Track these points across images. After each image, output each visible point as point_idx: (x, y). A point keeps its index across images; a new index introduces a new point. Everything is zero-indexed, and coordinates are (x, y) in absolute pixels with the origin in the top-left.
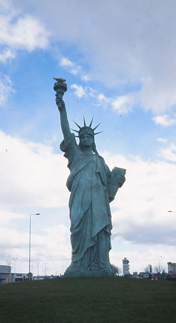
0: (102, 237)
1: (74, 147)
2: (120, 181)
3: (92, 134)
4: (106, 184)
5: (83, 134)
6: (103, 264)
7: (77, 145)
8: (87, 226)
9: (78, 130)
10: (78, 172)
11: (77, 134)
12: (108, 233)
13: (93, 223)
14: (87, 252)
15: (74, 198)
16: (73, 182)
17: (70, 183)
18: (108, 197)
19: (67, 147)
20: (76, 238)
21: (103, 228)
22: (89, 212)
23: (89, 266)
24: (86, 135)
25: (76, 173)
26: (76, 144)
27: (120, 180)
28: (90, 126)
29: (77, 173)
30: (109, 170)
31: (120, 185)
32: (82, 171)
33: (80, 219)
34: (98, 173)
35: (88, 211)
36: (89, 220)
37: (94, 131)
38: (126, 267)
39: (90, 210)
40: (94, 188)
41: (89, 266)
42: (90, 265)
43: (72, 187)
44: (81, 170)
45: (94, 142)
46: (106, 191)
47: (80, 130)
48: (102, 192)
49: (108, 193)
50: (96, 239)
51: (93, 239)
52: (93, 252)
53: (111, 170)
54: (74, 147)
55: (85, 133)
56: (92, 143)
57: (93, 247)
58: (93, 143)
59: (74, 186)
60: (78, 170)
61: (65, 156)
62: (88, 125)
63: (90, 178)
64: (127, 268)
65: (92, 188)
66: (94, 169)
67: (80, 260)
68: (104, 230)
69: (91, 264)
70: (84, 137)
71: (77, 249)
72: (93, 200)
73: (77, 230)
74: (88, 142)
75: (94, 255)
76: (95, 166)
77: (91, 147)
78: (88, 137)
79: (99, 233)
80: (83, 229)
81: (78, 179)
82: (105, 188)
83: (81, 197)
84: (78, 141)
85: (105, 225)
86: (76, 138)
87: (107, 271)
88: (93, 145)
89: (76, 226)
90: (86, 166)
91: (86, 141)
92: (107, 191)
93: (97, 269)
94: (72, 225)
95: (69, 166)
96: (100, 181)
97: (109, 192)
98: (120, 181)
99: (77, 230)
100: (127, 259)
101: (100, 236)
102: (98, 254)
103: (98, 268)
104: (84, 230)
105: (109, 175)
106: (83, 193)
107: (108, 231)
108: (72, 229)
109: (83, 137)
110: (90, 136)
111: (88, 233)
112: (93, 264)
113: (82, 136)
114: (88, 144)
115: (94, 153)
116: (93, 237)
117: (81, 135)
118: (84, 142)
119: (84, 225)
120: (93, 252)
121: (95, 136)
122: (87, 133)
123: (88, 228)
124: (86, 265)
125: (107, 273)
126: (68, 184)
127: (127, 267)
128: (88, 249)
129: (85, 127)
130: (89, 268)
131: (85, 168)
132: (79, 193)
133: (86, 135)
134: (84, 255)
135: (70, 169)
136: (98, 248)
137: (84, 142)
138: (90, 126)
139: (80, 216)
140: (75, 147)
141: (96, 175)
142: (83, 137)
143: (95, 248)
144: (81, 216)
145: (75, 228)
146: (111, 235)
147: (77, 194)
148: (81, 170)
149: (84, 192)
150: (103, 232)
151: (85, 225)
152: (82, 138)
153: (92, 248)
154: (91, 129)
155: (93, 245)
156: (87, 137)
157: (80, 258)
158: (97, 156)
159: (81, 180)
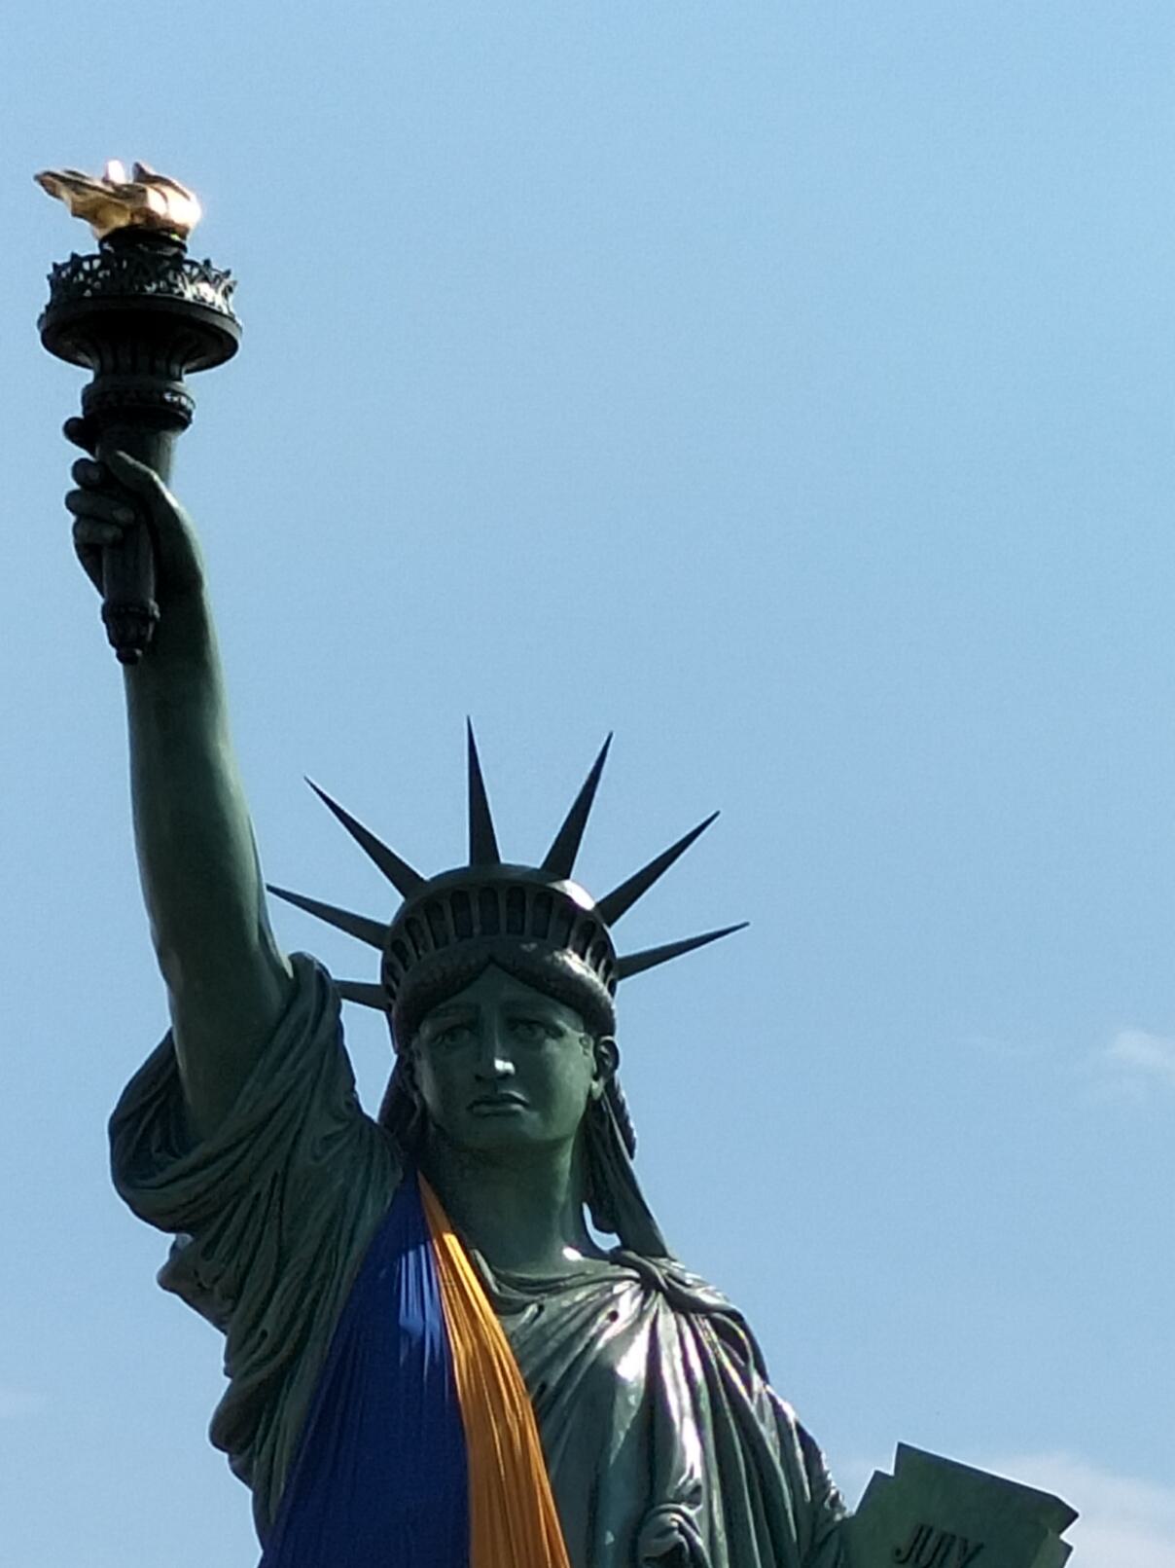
9: (384, 904)
28: (562, 857)
45: (611, 1088)
47: (405, 919)
53: (851, 1504)
61: (174, 1278)
62: (523, 847)
86: (352, 1014)
115: (608, 1242)
121: (631, 1003)
138: (562, 857)
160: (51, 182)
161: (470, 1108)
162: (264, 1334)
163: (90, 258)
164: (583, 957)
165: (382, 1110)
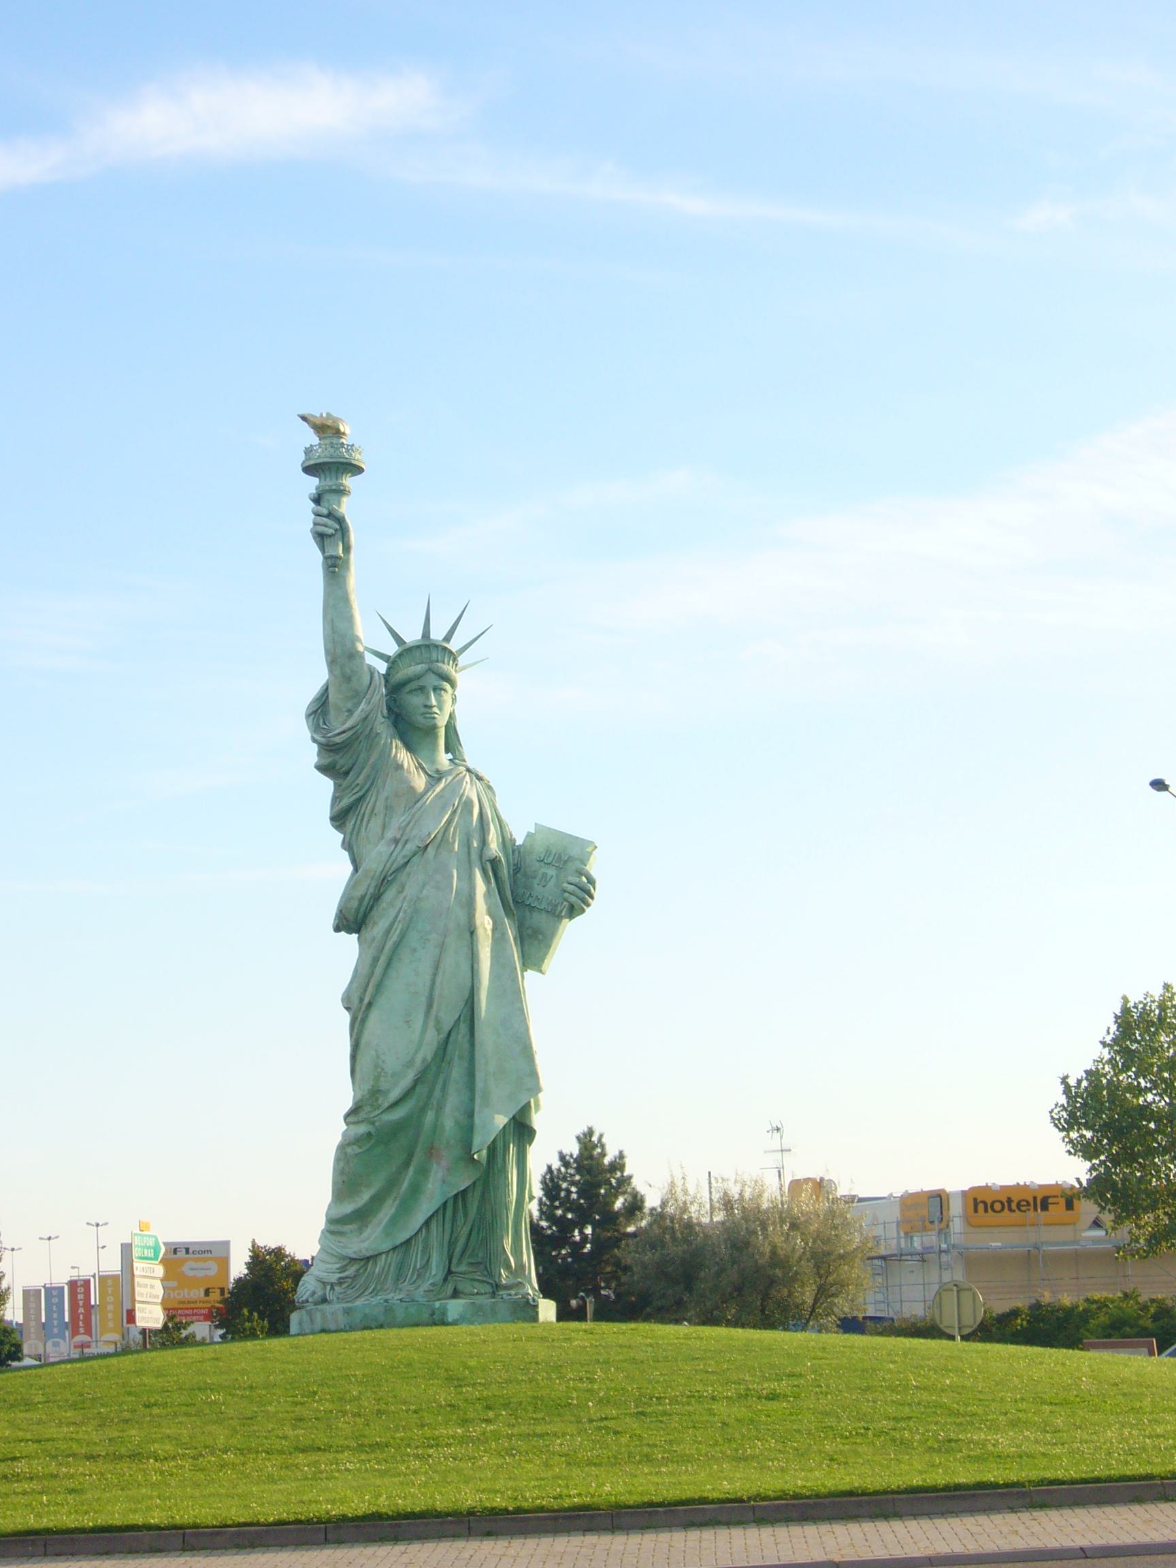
5: (418, 677)
15: (392, 973)
19: (350, 733)
25: (401, 861)
28: (447, 639)
32: (429, 849)
41: (445, 1280)
42: (450, 1272)
47: (400, 655)
52: (466, 1215)
57: (464, 1193)
60: (411, 847)
62: (437, 635)
69: (453, 1269)
75: (466, 1231)
80: (423, 1110)
81: (410, 891)
83: (425, 968)
89: (395, 1094)
104: (430, 1116)
111: (449, 1123)
112: (463, 1268)
113: (413, 685)
119: (430, 1096)
123: (448, 1109)
124: (436, 1271)
130: (449, 1289)
132: (415, 950)
134: (420, 1229)
138: (447, 639)
145: (386, 1105)
151: (437, 1093)
152: (411, 692)
157: (398, 1242)
159: (425, 892)
160: (304, 418)
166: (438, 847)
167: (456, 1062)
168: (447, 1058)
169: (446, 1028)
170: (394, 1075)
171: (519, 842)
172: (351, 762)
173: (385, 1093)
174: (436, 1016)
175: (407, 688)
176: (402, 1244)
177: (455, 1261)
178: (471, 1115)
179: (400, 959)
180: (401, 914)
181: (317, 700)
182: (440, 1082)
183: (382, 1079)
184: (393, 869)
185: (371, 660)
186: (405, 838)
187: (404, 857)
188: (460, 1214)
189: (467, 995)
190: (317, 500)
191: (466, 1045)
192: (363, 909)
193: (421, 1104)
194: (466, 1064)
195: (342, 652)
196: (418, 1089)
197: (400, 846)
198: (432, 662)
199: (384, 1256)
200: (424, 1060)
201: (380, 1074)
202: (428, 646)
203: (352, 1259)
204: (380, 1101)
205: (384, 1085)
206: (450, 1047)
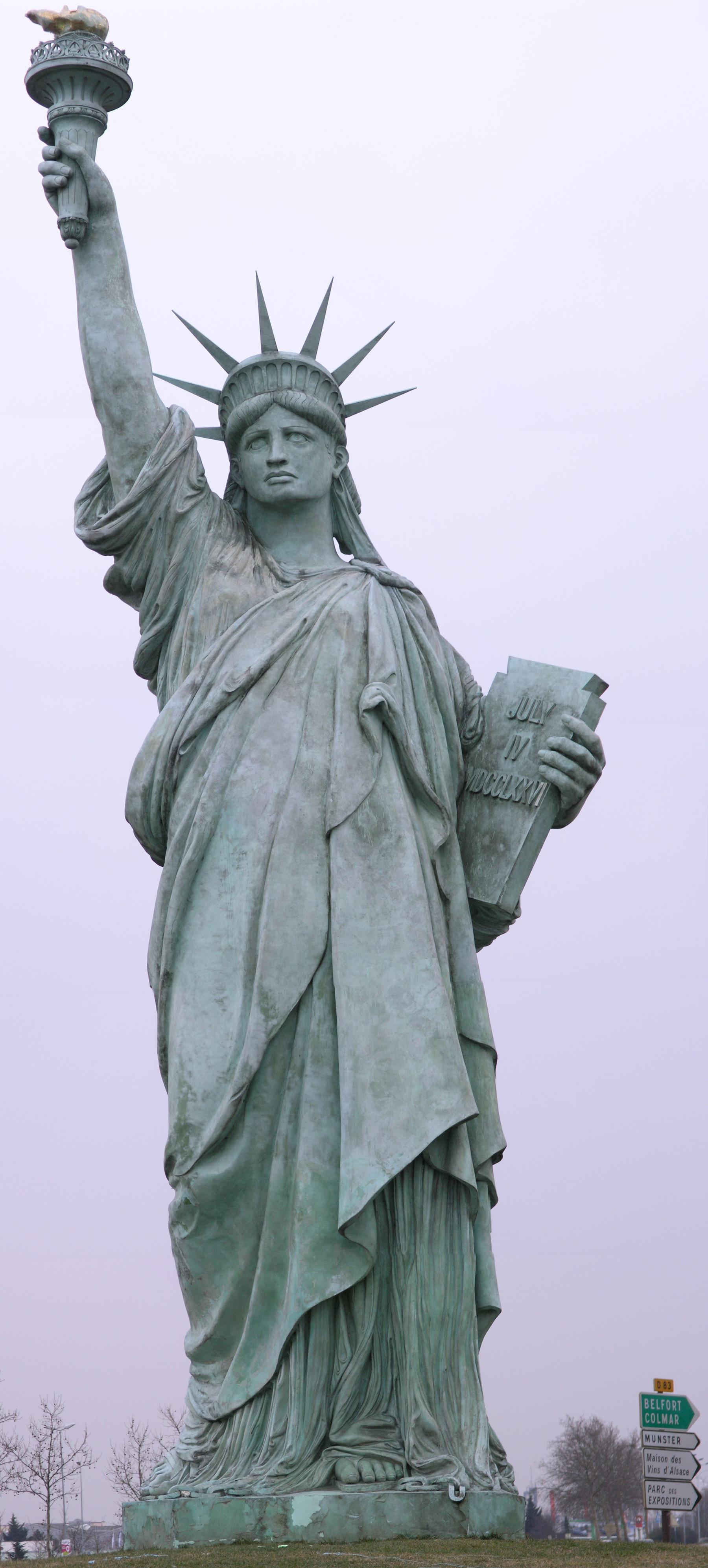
0: (415, 1223)
1: (181, 517)
2: (553, 774)
3: (323, 405)
4: (448, 799)
5: (256, 416)
6: (429, 1433)
7: (214, 496)
8: (296, 1130)
10: (222, 707)
11: (206, 414)
12: (466, 1187)
13: (345, 1106)
14: (301, 1334)
15: (194, 918)
16: (183, 788)
17: (154, 797)
18: (459, 900)
20: (210, 1232)
21: (424, 1145)
22: (314, 1018)
23: (317, 1456)
24: (277, 420)
26: (201, 488)
27: (552, 765)
29: (214, 717)
30: (468, 686)
31: (564, 808)
32: (250, 696)
33: (239, 1078)
34: (379, 710)
35: (302, 1018)
36: (312, 1086)
37: (343, 389)
38: (669, 1454)
39: (318, 1007)
40: (345, 833)
42: (325, 1443)
43: (176, 830)
44: (244, 690)
45: (345, 471)
46: (444, 849)
47: (230, 385)
48: (409, 868)
49: (459, 869)
50: (370, 1235)
51: (345, 1234)
52: (353, 1342)
54: (181, 517)
55: (268, 406)
56: (325, 481)
58: (335, 481)
59: (191, 816)
60: (215, 695)
62: (290, 344)
63: (315, 756)
64: (675, 1460)
65: (328, 836)
66: (348, 675)
67: (250, 1401)
68: (437, 1161)
69: (333, 1438)
70: (265, 436)
71: (224, 1316)
72: (335, 926)
73: (220, 1167)
74: (299, 468)
76: (349, 656)
77: (323, 511)
78: (297, 433)
79: (392, 1185)
82: (438, 832)
83: (241, 903)
84: (215, 463)
85: (436, 1129)
87: (457, 1489)
88: (334, 500)
89: (210, 1131)
90: (280, 663)
91: (283, 462)
92: (457, 857)
93: (380, 1474)
94: (182, 1130)
95: (148, 664)
96: (393, 779)
97: (467, 862)
98: (553, 774)
99: (220, 1167)
100: (677, 1391)
101: (403, 1212)
102: (382, 1358)
103: (388, 1466)
105: (472, 724)
106: (259, 869)
107: (465, 1172)
108: (179, 1159)
109: (256, 439)
110: (313, 430)
111: (304, 1183)
112: (351, 1435)
113: (250, 432)
114: (295, 488)
116: (341, 1223)
117: (243, 425)
118: (267, 471)
119: (273, 1131)
120: (353, 1342)
121: (353, 426)
122: (283, 406)
124: (294, 1445)
125: (458, 1503)
126: (138, 803)
127: (678, 1454)
128: (308, 1316)
129: (271, 361)
130: (320, 1472)
131: (272, 675)
132: (225, 873)
133: (277, 420)
135: (153, 688)
136: (387, 1310)
137: (267, 471)
139: (237, 1053)
140: (193, 517)
141: (363, 729)
142: (256, 439)
143: (367, 1311)
144: (251, 1055)
145: (199, 1150)
146: (494, 1200)
147: (210, 882)
148: (244, 690)
149: (266, 862)
150: (427, 1181)
151: (284, 1126)
152: (249, 446)
153: (342, 1312)
154: (317, 372)
155: (347, 1286)
156: (287, 434)
157: (253, 1392)
158: (372, 581)
159: (241, 770)
161: (265, 481)
162: (157, 605)
163: (49, 43)
164: (325, 401)
165: (225, 494)
166: (270, 694)
167: (309, 1069)
168: (297, 1062)
169: (285, 1006)
170: (206, 1096)
171: (485, 693)
172: (142, 565)
173: (197, 1129)
174: (260, 987)
175: (244, 443)
176: (259, 1395)
177: (337, 1423)
178: (335, 1159)
179: (203, 891)
180: (199, 813)
181: (96, 474)
182: (287, 1106)
183: (190, 1105)
184: (186, 736)
185: (169, 396)
186: (208, 680)
187: (204, 711)
188: (344, 1341)
189: (321, 948)
190: (48, 136)
191: (326, 1038)
192: (153, 811)
193: (261, 1146)
194: (328, 1071)
195: (117, 389)
196: (250, 1120)
197: (198, 696)
198: (279, 389)
199: (238, 1415)
200: (246, 1065)
201: (186, 1095)
202: (271, 364)
203: (211, 1422)
204: (191, 1146)
205: (193, 1118)
206: (299, 1042)
